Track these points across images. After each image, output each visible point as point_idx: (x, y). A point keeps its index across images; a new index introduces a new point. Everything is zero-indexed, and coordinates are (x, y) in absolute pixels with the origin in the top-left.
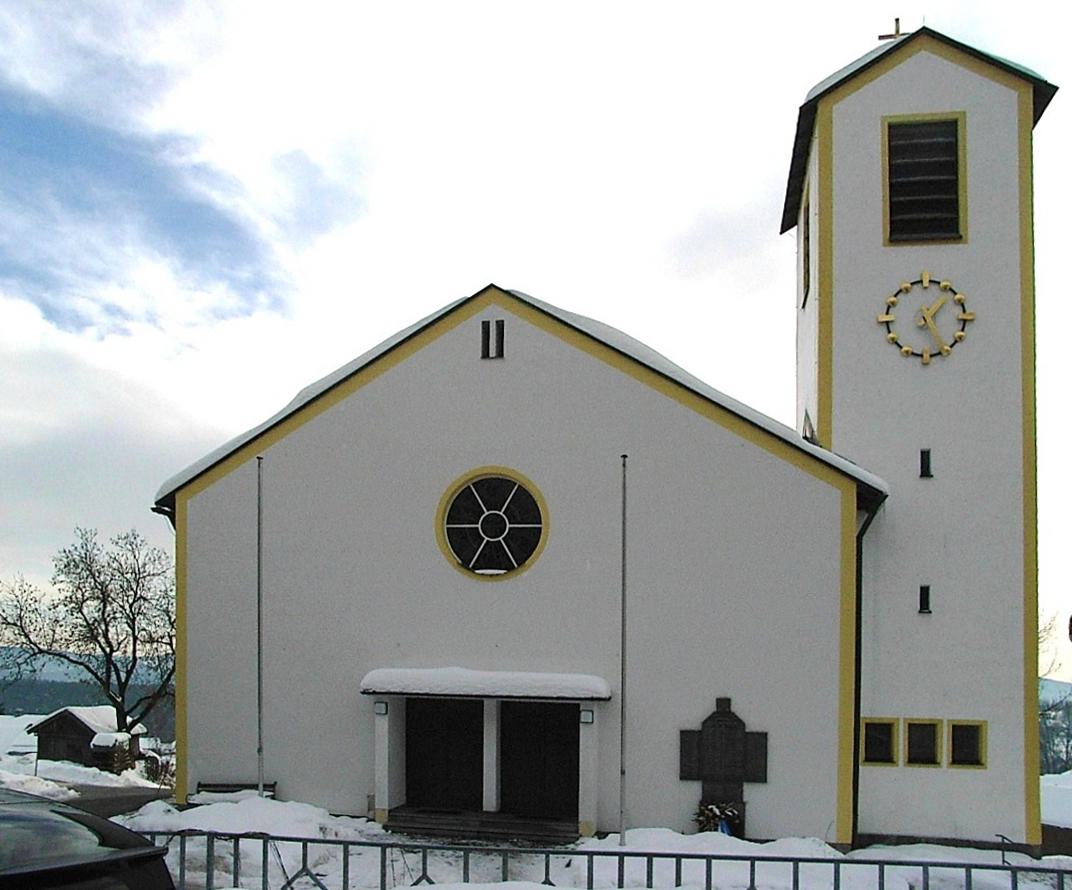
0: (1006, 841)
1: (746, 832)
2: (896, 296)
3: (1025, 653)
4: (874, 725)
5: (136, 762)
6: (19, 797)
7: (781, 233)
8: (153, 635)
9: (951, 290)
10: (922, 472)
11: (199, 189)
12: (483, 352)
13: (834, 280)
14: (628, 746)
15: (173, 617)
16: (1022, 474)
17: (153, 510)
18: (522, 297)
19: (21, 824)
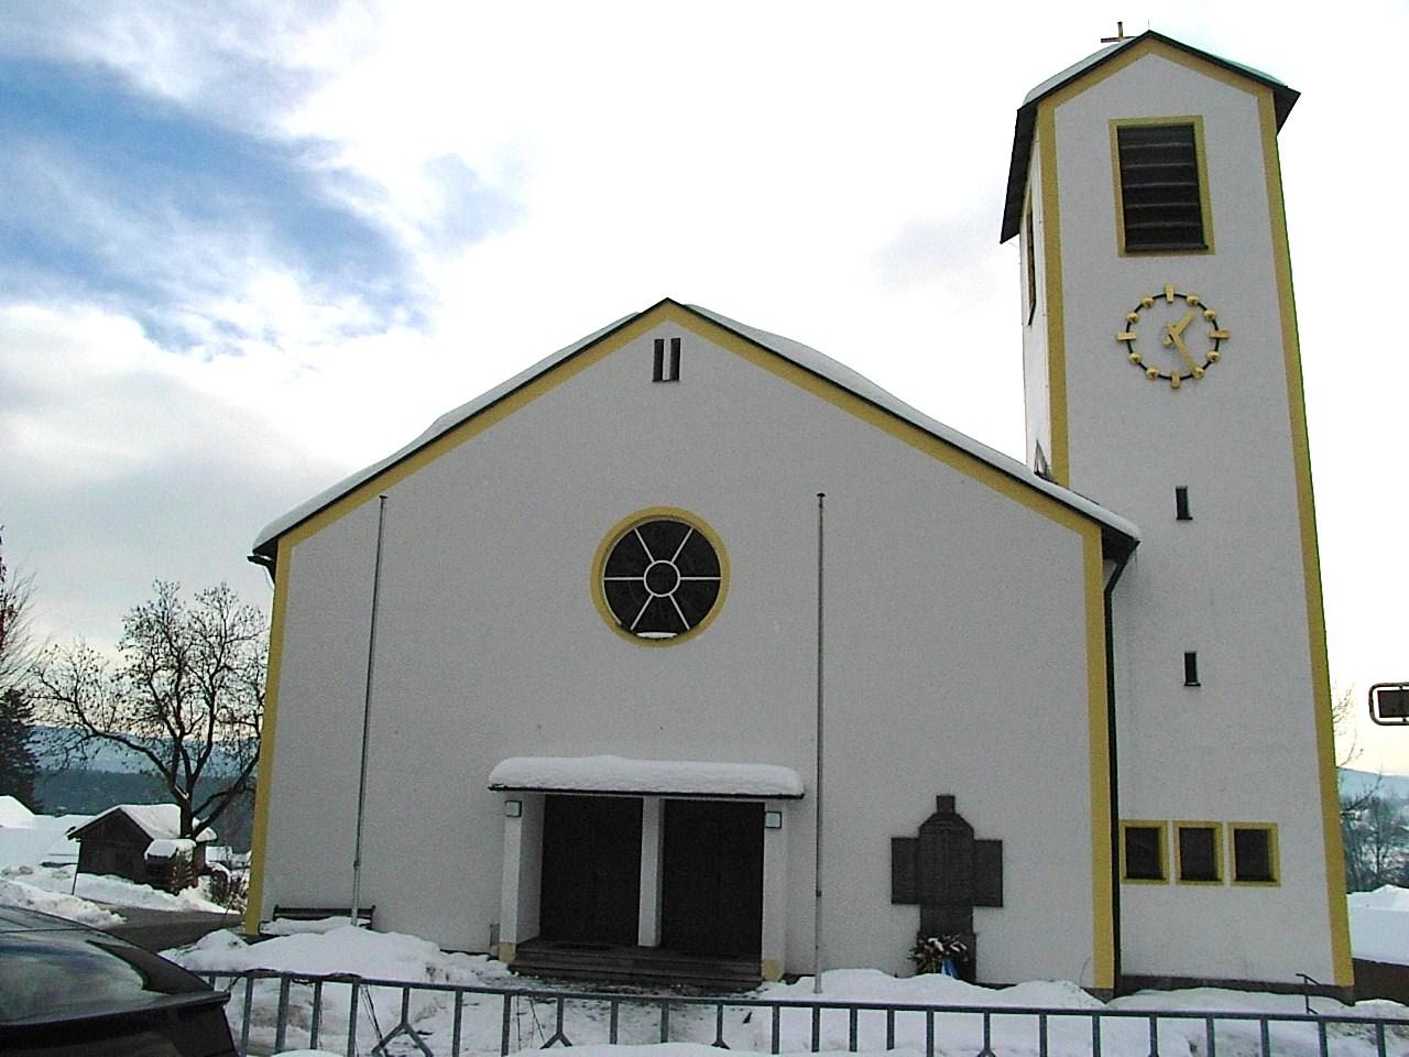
0: (1309, 982)
1: (978, 975)
2: (1136, 311)
3: (1318, 736)
4: (1137, 829)
5: (200, 879)
6: (49, 921)
7: (1001, 242)
8: (236, 715)
9: (1199, 304)
10: (1179, 514)
11: (338, 195)
12: (655, 374)
13: (1064, 294)
14: (825, 857)
15: (262, 692)
16: (1297, 515)
17: (250, 559)
18: (702, 312)
19: (49, 957)
